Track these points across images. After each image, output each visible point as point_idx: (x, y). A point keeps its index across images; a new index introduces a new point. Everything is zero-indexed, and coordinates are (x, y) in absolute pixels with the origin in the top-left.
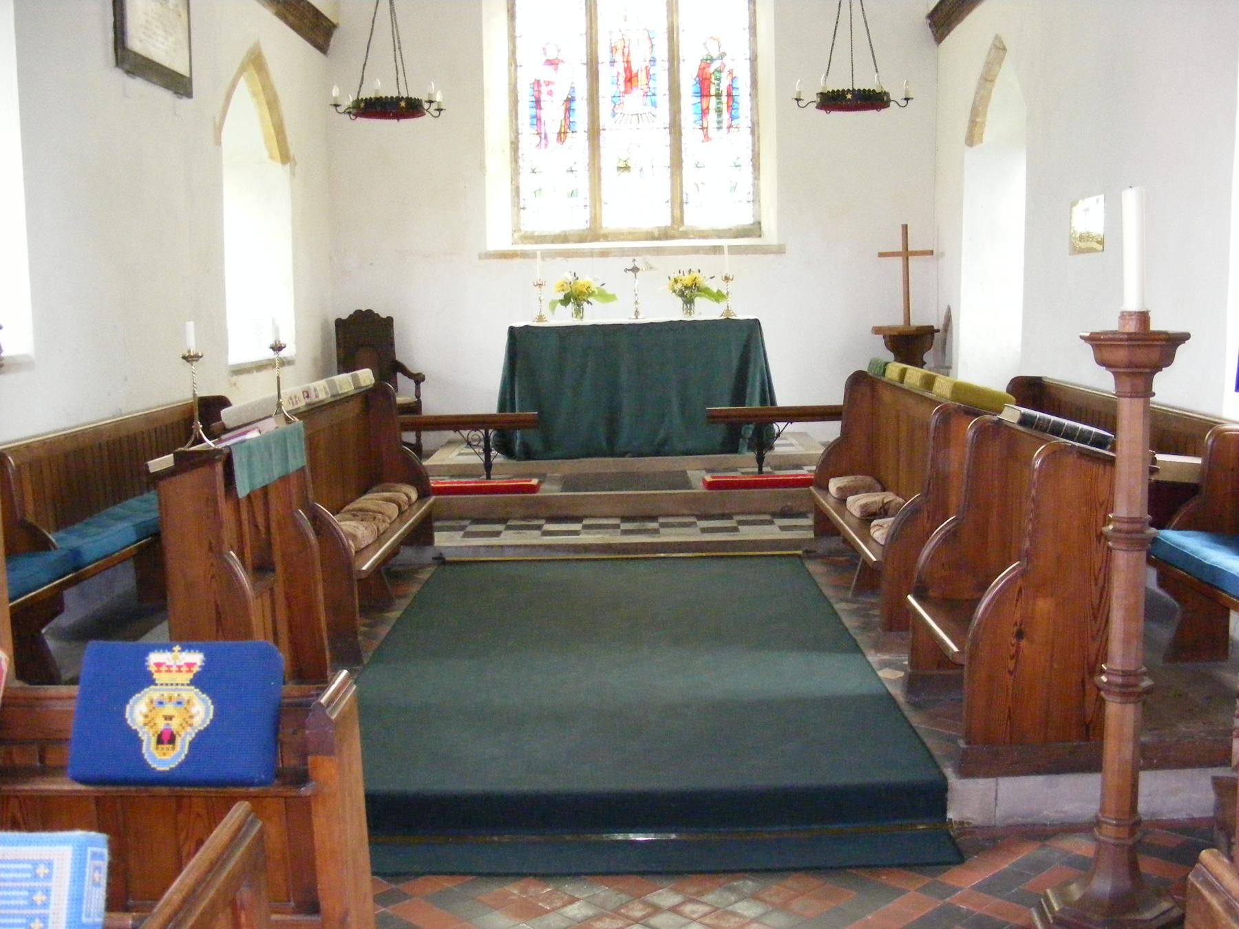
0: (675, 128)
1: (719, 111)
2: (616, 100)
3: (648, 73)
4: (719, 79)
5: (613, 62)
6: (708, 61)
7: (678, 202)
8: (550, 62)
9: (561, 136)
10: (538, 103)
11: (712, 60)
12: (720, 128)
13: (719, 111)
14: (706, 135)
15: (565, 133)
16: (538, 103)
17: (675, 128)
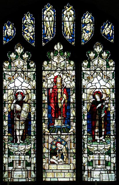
0: (79, 134)
1: (100, 129)
2: (51, 122)
3: (66, 109)
4: (101, 113)
5: (49, 103)
6: (95, 103)
7: (79, 169)
8: (18, 102)
9: (23, 138)
10: (12, 123)
11: (98, 103)
12: (100, 136)
13: (100, 129)
14: (94, 138)
15: (26, 136)
16: (12, 123)
17: (79, 134)
